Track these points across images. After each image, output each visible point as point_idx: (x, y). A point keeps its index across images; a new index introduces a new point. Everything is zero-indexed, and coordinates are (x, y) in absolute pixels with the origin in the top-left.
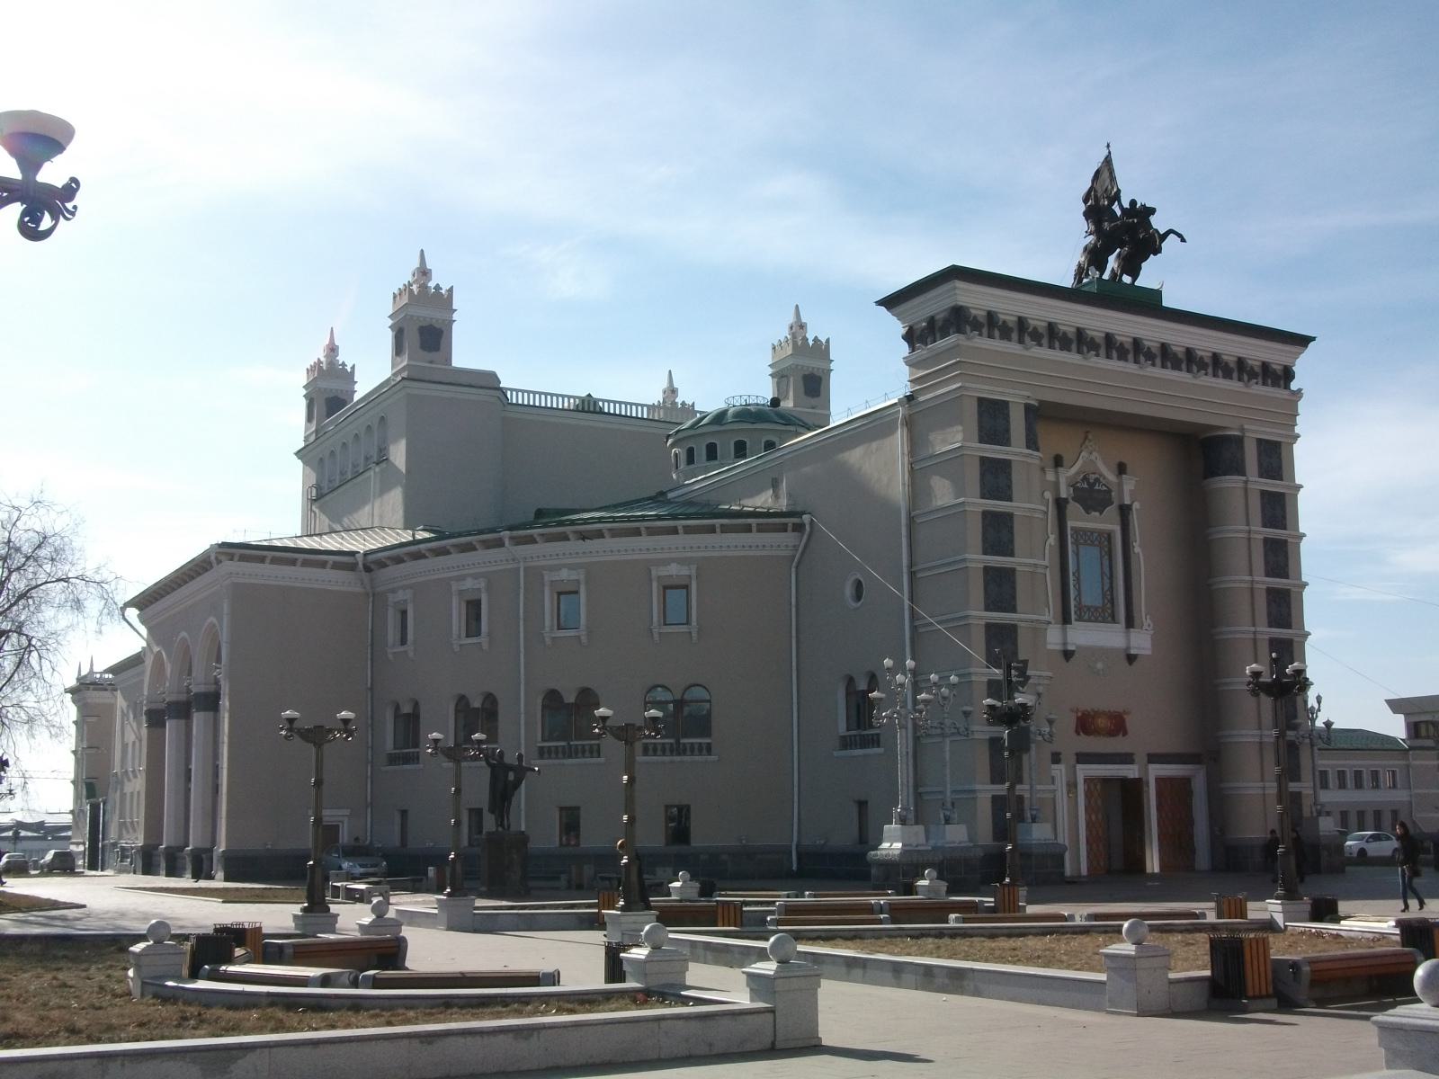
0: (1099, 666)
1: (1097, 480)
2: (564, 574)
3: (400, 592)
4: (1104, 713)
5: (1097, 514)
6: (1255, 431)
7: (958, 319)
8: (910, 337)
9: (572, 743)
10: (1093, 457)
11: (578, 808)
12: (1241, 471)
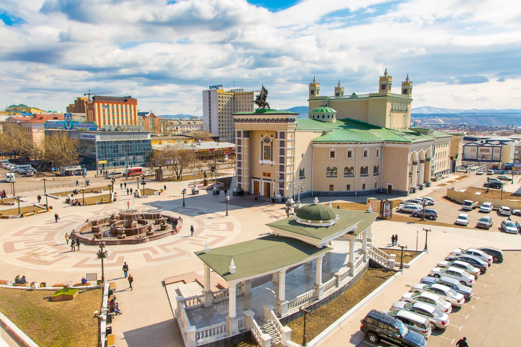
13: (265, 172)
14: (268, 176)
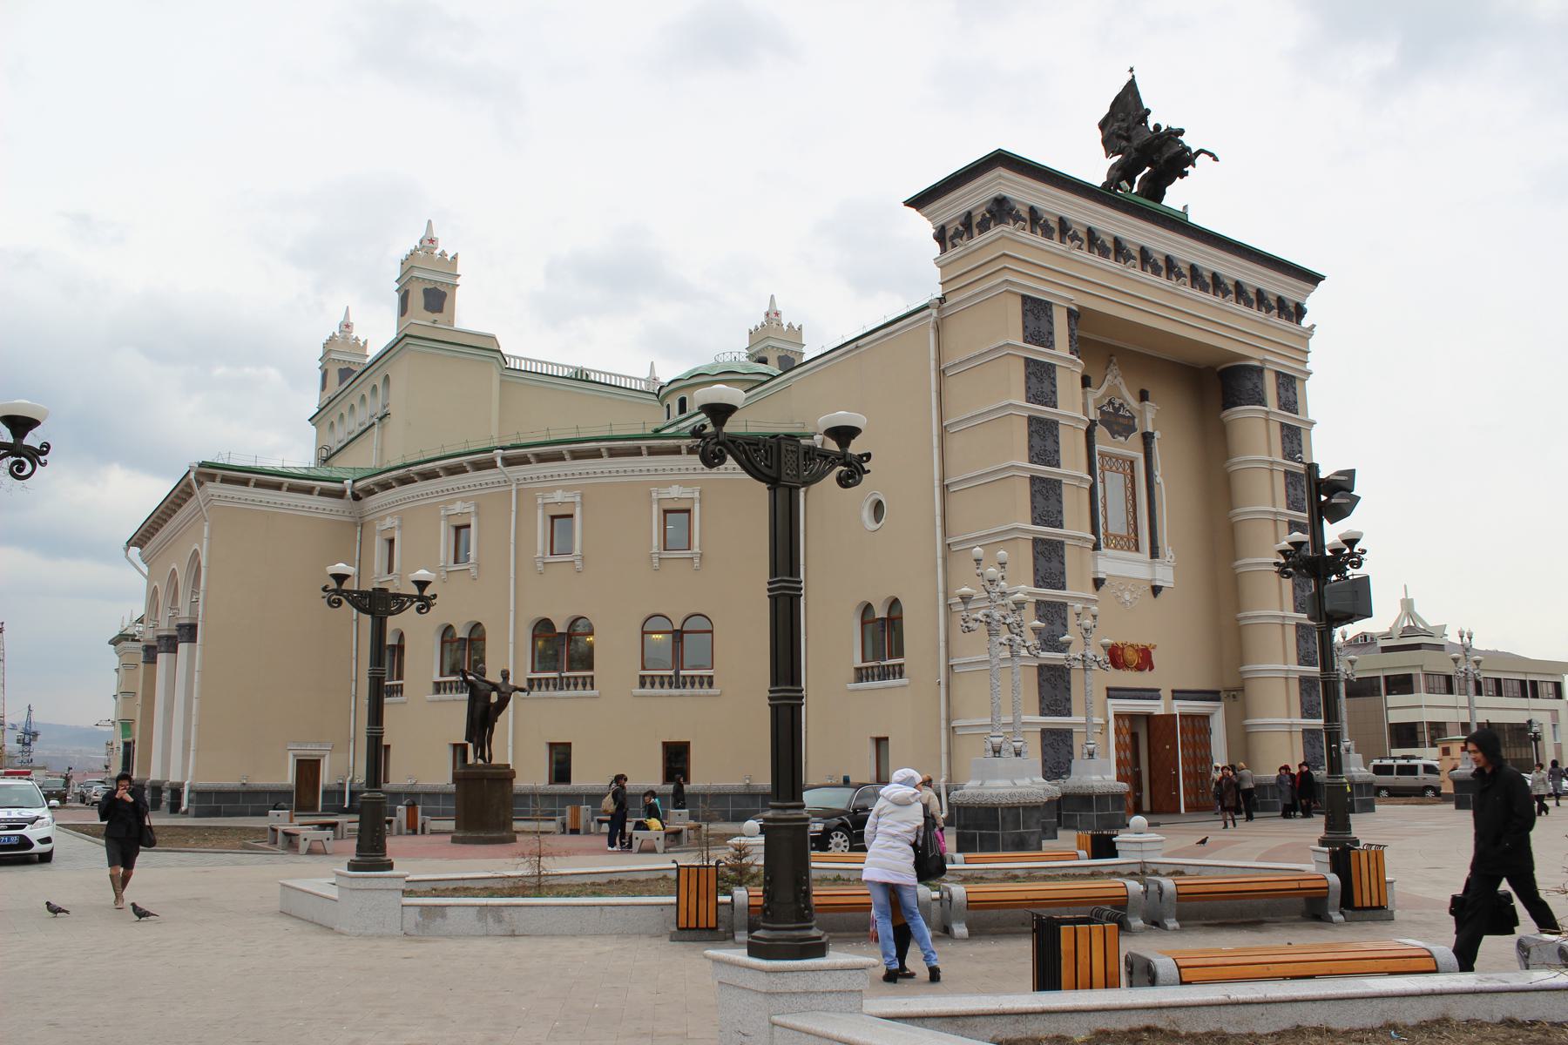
0: (1127, 596)
1: (1121, 405)
2: (558, 496)
3: (388, 519)
4: (1132, 646)
5: (1122, 439)
6: (1275, 362)
7: (1001, 210)
8: (941, 236)
9: (563, 674)
10: (1116, 382)
11: (569, 745)
12: (1261, 401)
13: (1119, 639)
14: (1139, 668)
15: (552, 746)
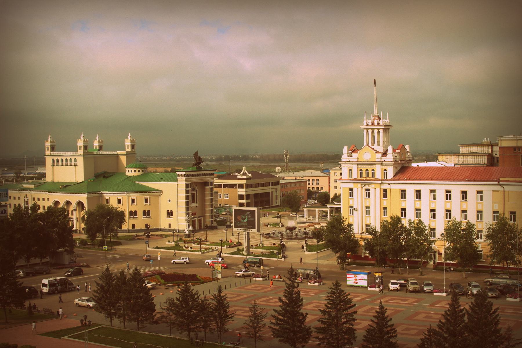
14: (195, 215)
15: (133, 225)
